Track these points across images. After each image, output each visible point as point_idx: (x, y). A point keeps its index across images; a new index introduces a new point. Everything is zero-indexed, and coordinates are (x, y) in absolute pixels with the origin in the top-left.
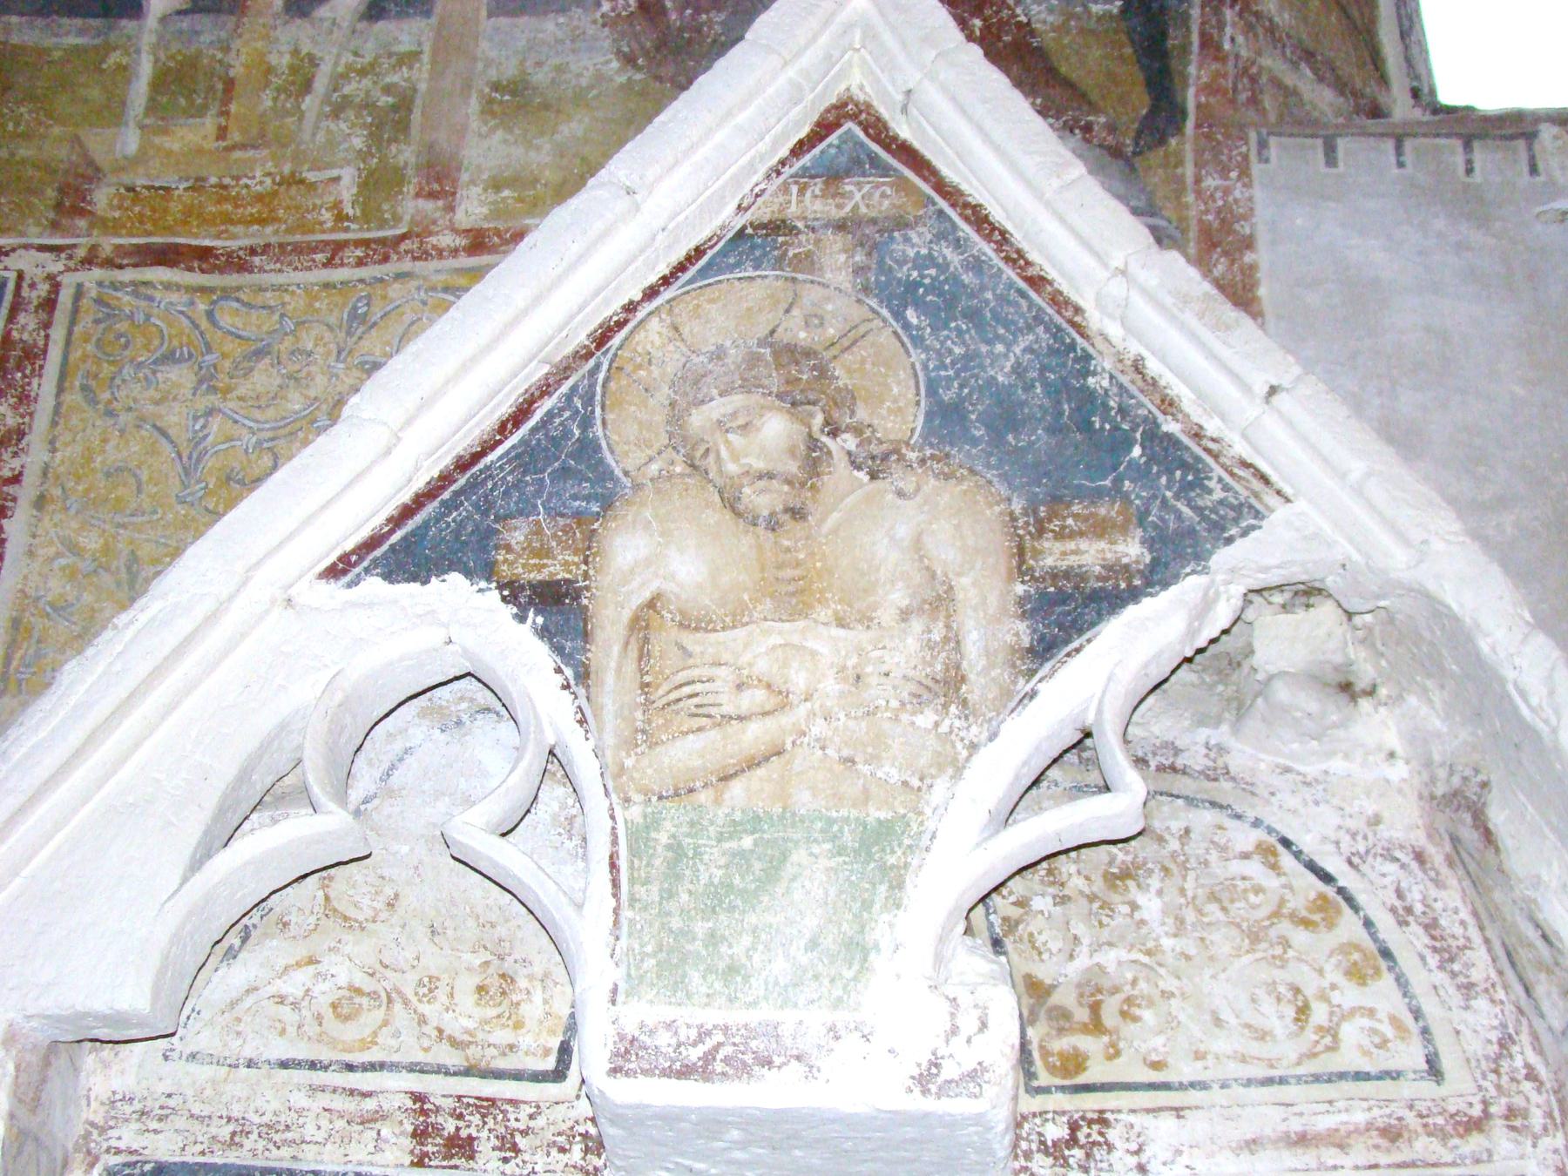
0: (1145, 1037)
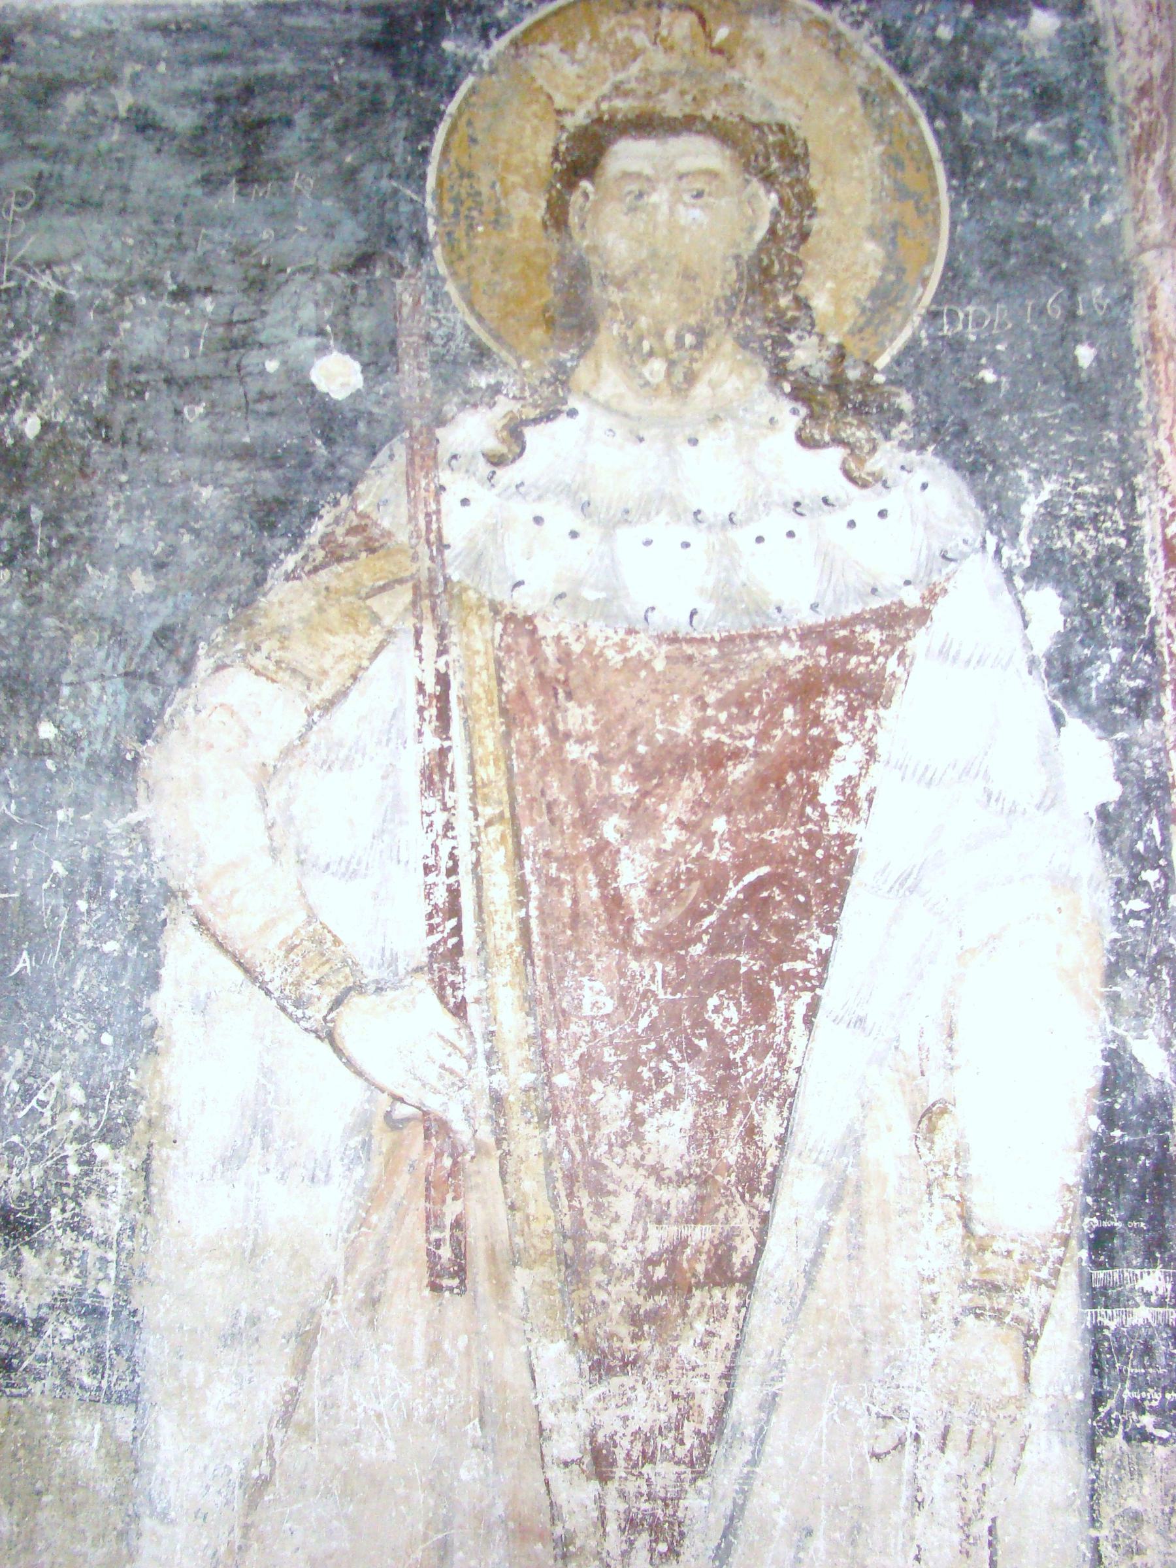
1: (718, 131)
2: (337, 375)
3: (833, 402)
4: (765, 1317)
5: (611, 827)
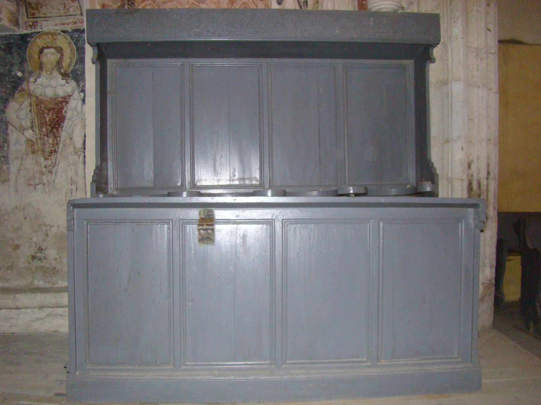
0: (44, 10)
1: (54, 48)
2: (20, 74)
3: (65, 75)
4: (58, 155)
5: (45, 115)
